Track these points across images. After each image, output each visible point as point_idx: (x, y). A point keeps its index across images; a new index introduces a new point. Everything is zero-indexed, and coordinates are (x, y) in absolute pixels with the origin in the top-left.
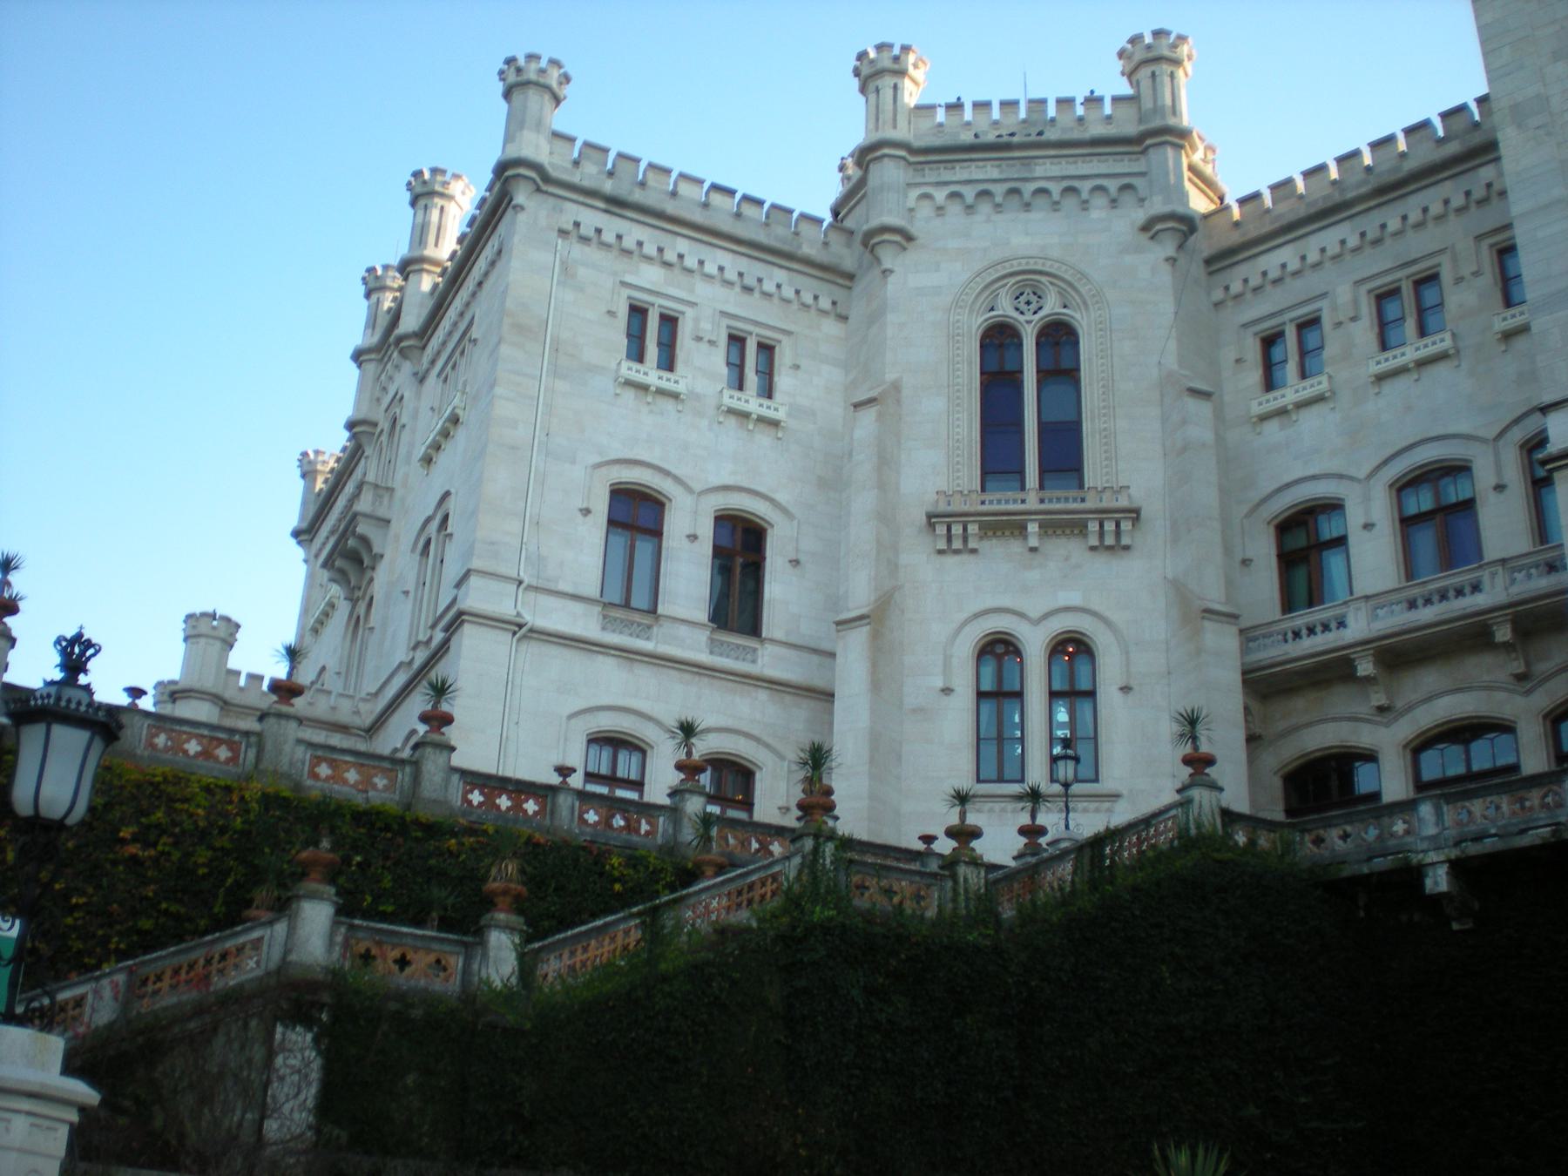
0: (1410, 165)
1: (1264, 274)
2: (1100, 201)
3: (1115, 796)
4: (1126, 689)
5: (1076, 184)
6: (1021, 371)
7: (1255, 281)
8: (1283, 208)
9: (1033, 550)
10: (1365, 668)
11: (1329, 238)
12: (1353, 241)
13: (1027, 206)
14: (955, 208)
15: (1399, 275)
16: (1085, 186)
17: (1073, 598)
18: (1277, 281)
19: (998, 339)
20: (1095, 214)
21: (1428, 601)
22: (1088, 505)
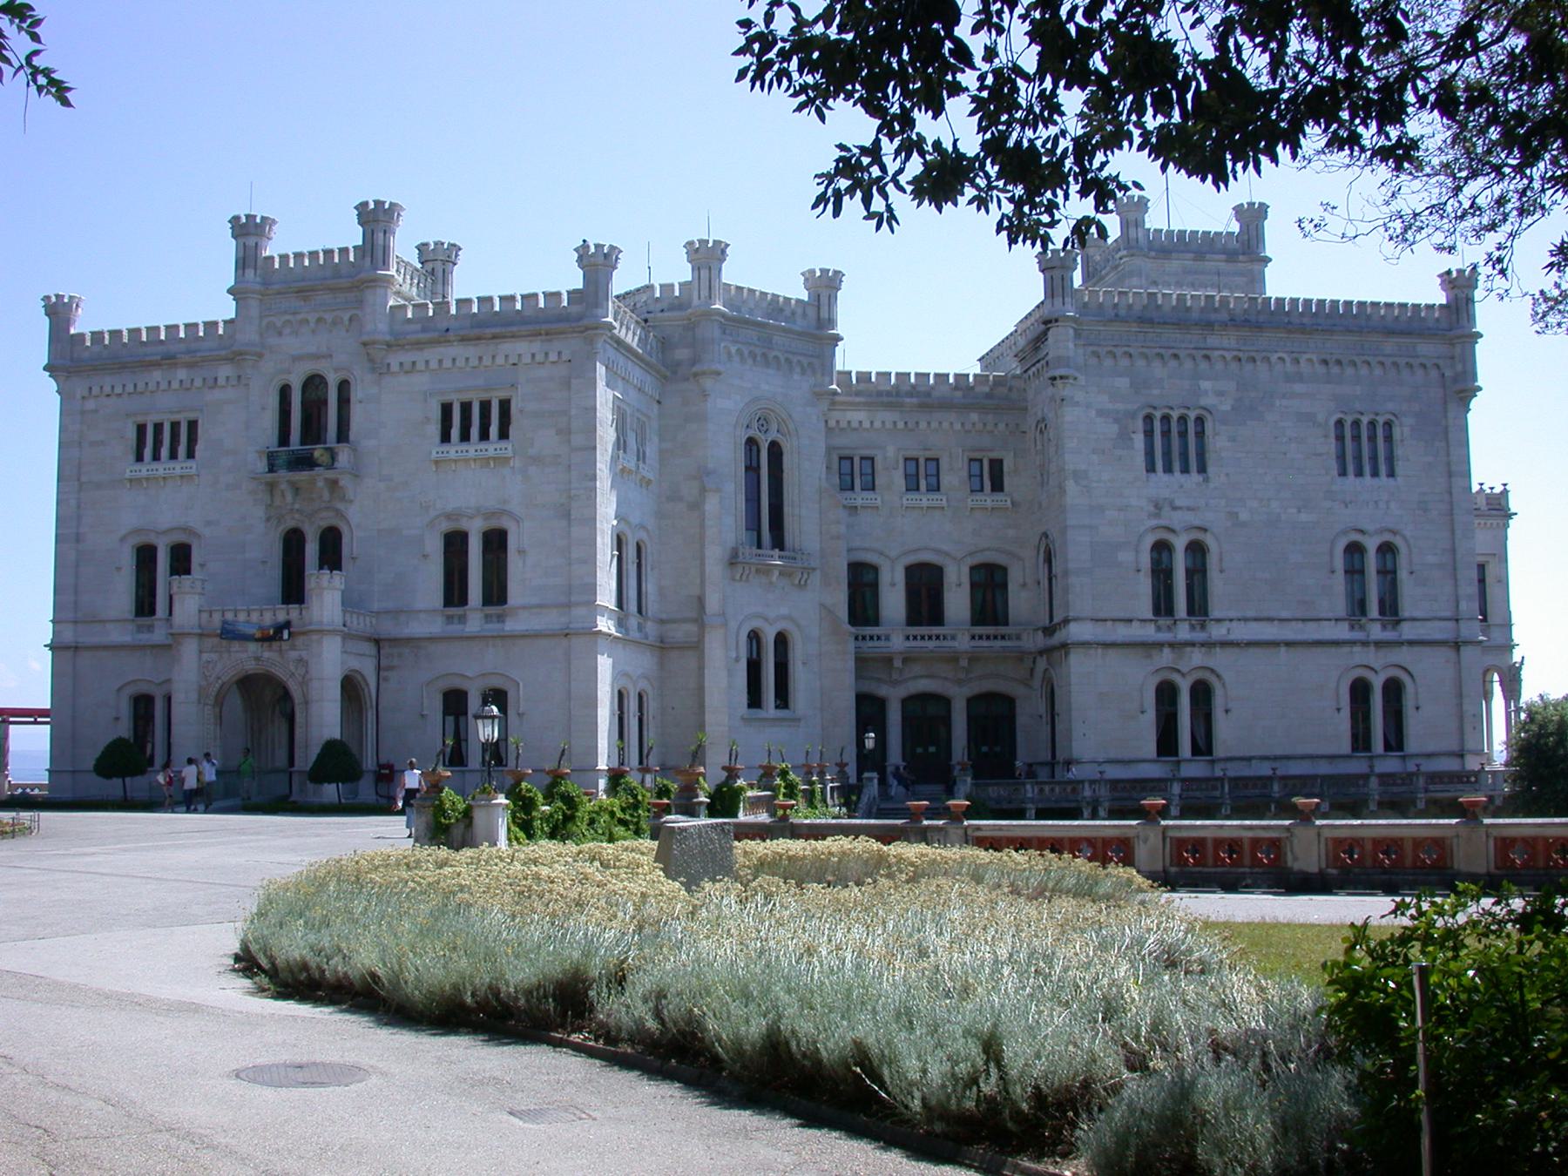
0: (936, 394)
1: (849, 422)
2: (798, 370)
3: (799, 720)
4: (804, 664)
5: (790, 356)
6: (759, 466)
7: (843, 424)
8: (862, 386)
9: (771, 583)
10: (897, 663)
11: (889, 417)
12: (901, 425)
13: (767, 364)
14: (736, 359)
15: (921, 453)
16: (795, 359)
17: (784, 611)
18: (855, 429)
19: (751, 443)
20: (796, 377)
21: (930, 638)
22: (800, 565)
